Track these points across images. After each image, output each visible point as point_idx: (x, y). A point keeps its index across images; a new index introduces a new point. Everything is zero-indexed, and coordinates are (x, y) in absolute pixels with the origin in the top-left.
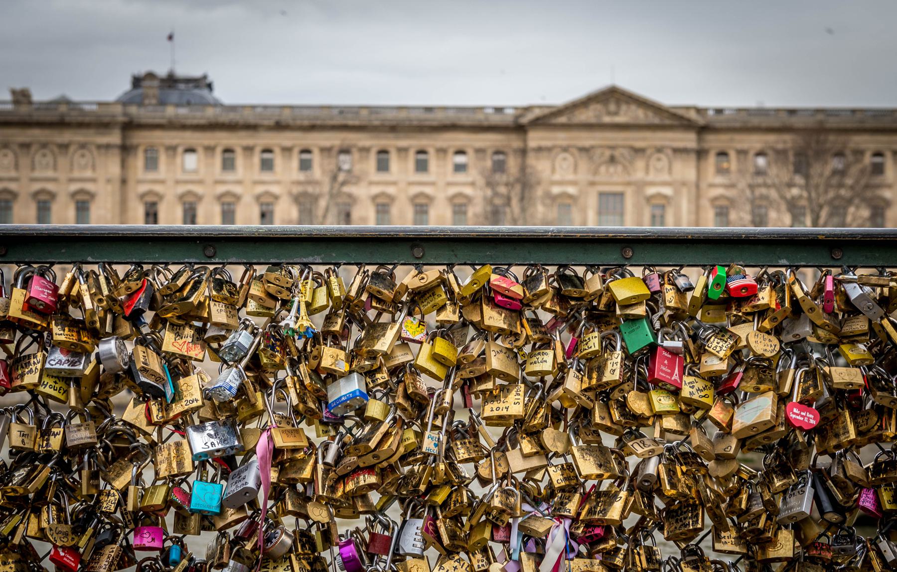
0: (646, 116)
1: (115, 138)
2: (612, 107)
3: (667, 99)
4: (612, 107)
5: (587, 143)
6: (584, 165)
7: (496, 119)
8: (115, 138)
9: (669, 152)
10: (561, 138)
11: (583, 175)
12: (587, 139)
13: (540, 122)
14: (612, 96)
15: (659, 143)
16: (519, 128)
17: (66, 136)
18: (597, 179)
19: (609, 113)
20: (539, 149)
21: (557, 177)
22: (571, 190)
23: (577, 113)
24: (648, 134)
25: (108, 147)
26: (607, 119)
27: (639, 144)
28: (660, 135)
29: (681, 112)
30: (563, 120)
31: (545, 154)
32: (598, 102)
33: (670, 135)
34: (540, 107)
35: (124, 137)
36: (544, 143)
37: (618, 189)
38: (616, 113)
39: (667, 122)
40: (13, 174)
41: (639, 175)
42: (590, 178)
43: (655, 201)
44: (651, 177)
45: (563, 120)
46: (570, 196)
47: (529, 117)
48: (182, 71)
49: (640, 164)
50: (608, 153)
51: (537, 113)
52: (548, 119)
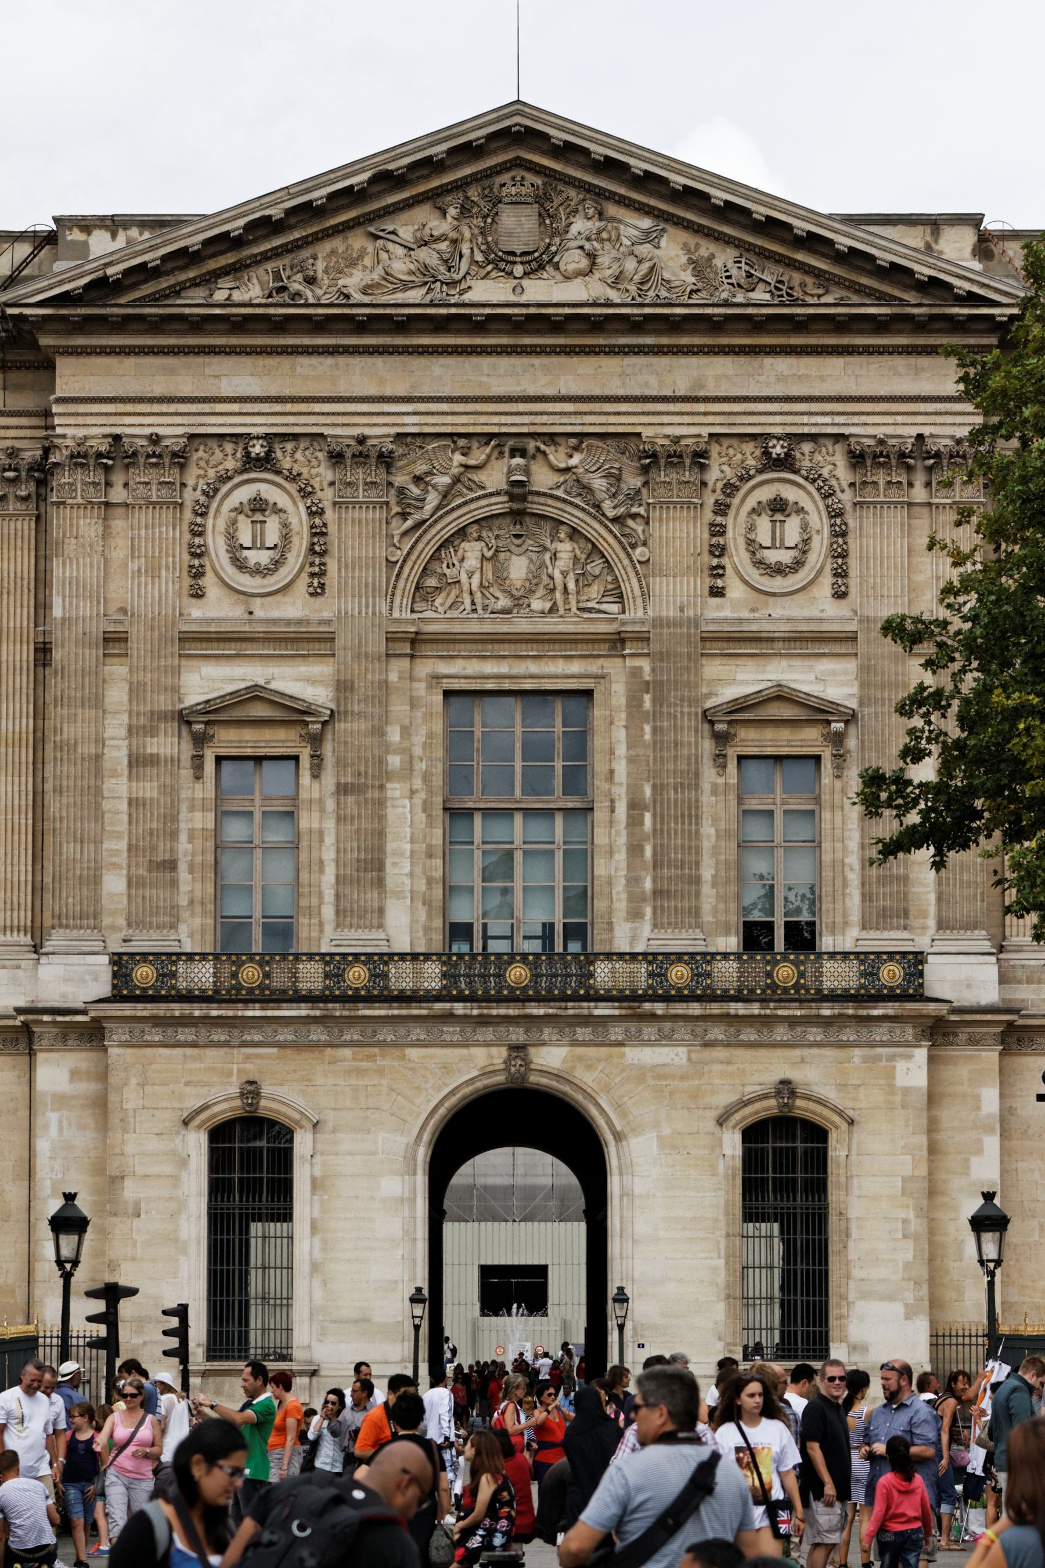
0: (699, 267)
2: (518, 228)
4: (518, 228)
5: (378, 428)
6: (360, 539)
9: (836, 466)
11: (357, 602)
13: (117, 308)
14: (517, 162)
15: (776, 422)
18: (437, 616)
19: (500, 261)
20: (116, 455)
21: (216, 608)
22: (304, 681)
23: (321, 259)
24: (719, 374)
26: (489, 292)
27: (660, 428)
28: (777, 374)
31: (146, 478)
32: (434, 198)
33: (834, 375)
34: (114, 224)
36: (136, 427)
37: (561, 670)
38: (538, 263)
39: (829, 302)
41: (673, 594)
43: (751, 740)
44: (734, 608)
45: (250, 292)
46: (295, 714)
47: (63, 274)
49: (677, 534)
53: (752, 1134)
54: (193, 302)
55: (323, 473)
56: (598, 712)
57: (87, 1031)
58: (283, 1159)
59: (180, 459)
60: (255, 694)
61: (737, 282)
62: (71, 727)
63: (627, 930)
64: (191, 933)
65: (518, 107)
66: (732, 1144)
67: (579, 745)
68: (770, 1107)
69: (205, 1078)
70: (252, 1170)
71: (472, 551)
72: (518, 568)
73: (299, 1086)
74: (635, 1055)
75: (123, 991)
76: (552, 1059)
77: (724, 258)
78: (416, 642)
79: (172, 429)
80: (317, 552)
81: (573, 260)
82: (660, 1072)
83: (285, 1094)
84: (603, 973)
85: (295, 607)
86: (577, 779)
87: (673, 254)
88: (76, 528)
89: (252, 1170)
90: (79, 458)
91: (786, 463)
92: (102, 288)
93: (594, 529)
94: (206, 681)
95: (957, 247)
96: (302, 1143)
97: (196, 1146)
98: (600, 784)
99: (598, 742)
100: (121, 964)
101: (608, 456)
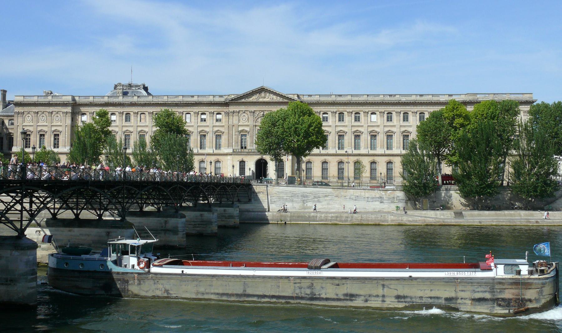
1: (69, 109)
2: (263, 94)
3: (284, 93)
6: (251, 118)
7: (217, 99)
8: (69, 109)
10: (243, 108)
11: (251, 123)
12: (252, 108)
16: (226, 104)
17: (51, 109)
19: (262, 97)
20: (234, 112)
22: (247, 129)
25: (67, 113)
26: (261, 100)
29: (290, 96)
31: (236, 114)
35: (73, 109)
36: (235, 110)
40: (31, 124)
42: (255, 124)
48: (134, 82)
50: (262, 113)
51: (233, 96)
52: (236, 101)
54: (239, 101)
57: (231, 155)
59: (239, 112)
60: (243, 130)
61: (279, 99)
62: (231, 132)
64: (239, 147)
69: (240, 158)
70: (242, 164)
73: (246, 158)
75: (234, 152)
78: (256, 126)
79: (238, 110)
80: (248, 119)
83: (245, 159)
85: (246, 123)
87: (275, 97)
88: (231, 117)
89: (242, 164)
90: (231, 112)
92: (232, 100)
94: (240, 129)
95: (296, 97)
97: (238, 163)
100: (233, 150)
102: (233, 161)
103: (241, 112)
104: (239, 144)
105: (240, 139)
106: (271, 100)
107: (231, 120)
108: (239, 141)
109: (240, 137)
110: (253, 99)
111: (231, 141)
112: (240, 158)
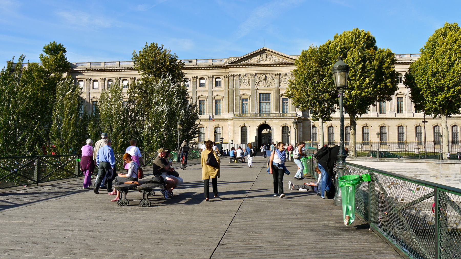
0: (279, 60)
2: (264, 56)
7: (216, 63)
16: (225, 67)
26: (262, 62)
30: (243, 63)
36: (236, 73)
38: (266, 60)
51: (232, 59)
53: (283, 127)
54: (239, 64)
55: (250, 76)
56: (271, 95)
58: (247, 129)
62: (231, 96)
63: (274, 111)
65: (264, 48)
66: (281, 128)
67: (269, 97)
68: (285, 125)
69: (241, 123)
71: (261, 82)
72: (265, 83)
74: (274, 121)
75: (235, 116)
76: (268, 122)
77: (281, 59)
81: (269, 59)
82: (275, 123)
84: (271, 115)
85: (248, 87)
86: (269, 100)
87: (277, 58)
91: (286, 75)
92: (232, 63)
93: (271, 81)
96: (248, 128)
97: (240, 129)
98: (271, 100)
99: (271, 97)
100: (234, 115)
101: (271, 74)
102: (234, 127)
103: (242, 76)
104: (240, 109)
105: (241, 103)
106: (273, 63)
107: (231, 84)
108: (240, 106)
109: (240, 101)
110: (254, 61)
111: (231, 106)
112: (241, 123)
